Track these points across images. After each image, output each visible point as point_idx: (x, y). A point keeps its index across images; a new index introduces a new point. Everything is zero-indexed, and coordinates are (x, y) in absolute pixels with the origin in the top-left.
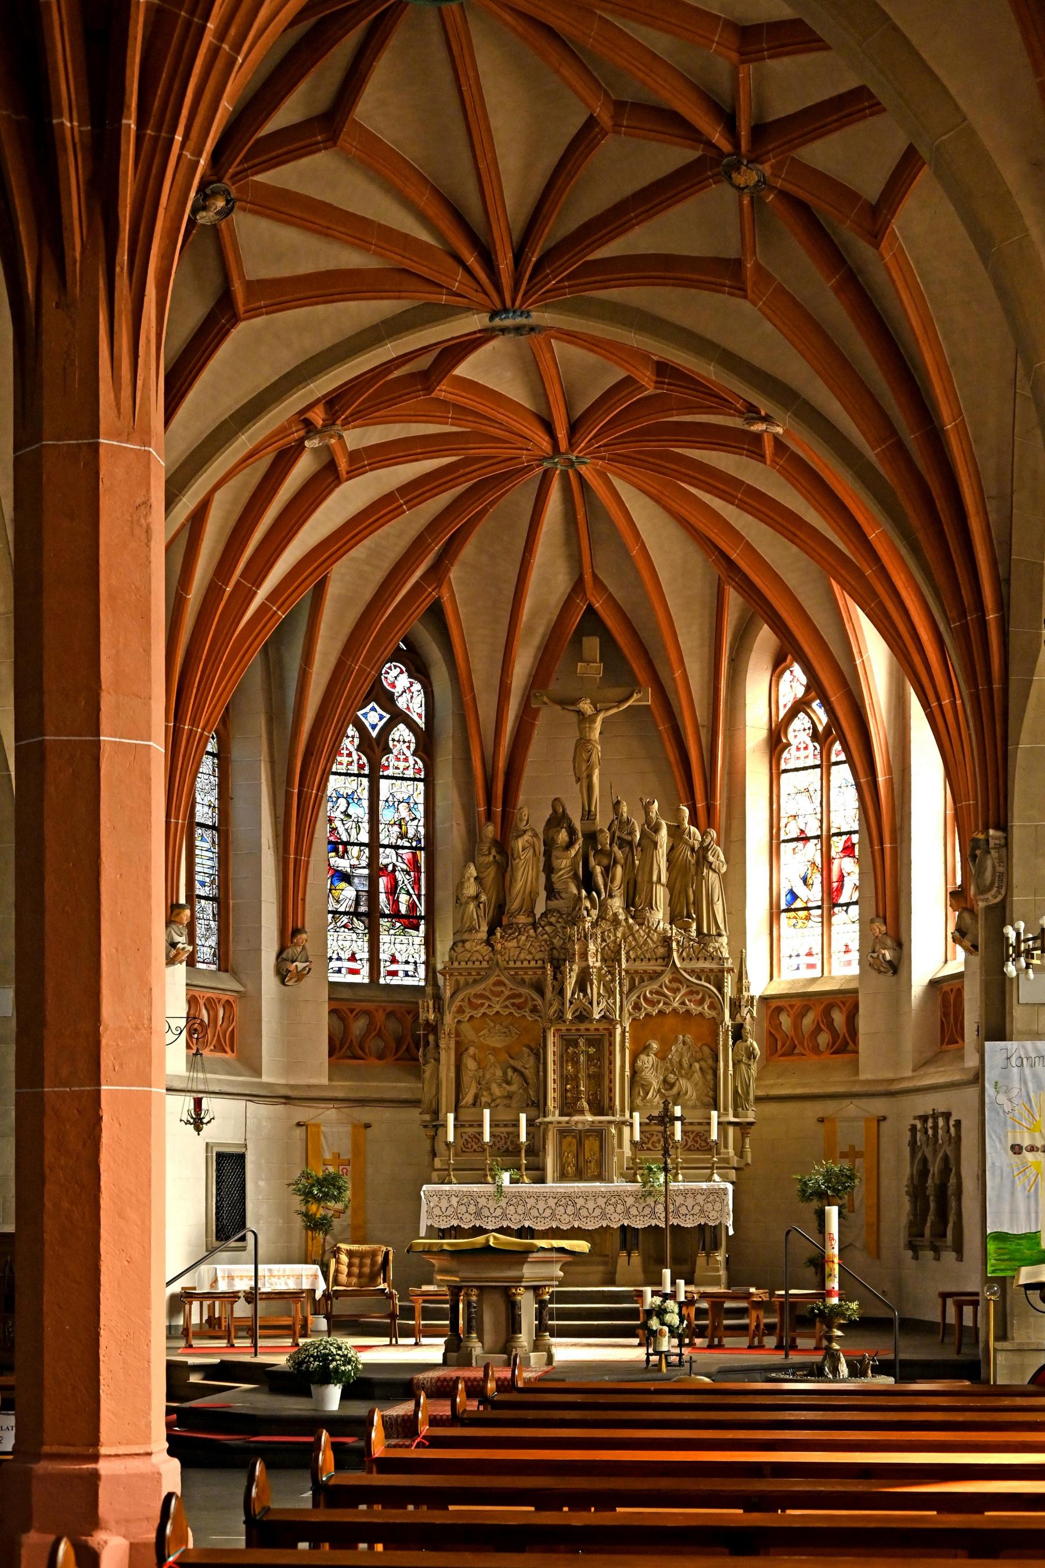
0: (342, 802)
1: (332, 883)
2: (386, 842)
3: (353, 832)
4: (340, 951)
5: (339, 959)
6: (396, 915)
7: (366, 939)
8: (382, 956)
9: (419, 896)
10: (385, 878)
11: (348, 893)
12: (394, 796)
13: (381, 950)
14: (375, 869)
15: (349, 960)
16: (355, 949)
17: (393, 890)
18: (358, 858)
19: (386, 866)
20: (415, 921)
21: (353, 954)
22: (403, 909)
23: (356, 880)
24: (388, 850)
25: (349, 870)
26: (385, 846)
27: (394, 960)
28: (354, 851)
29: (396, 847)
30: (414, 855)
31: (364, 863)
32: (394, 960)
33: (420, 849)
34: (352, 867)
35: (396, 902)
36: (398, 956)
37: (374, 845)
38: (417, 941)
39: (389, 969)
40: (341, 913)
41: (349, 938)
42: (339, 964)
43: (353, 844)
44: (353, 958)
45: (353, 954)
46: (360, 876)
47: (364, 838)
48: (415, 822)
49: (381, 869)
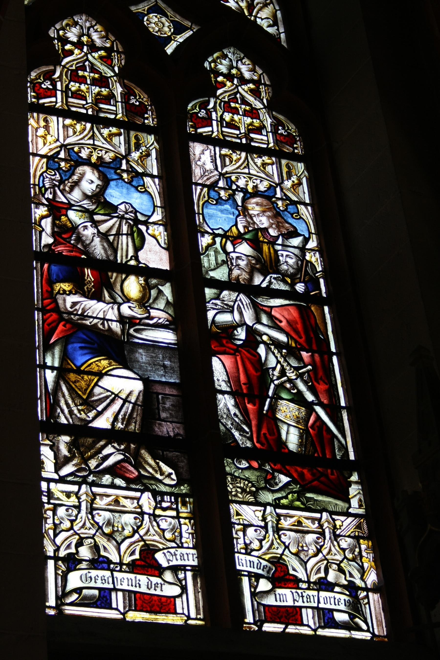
0: (90, 180)
1: (65, 357)
2: (220, 274)
3: (125, 243)
4: (101, 541)
5: (99, 562)
6: (270, 452)
7: (184, 511)
8: (243, 563)
9: (334, 411)
10: (228, 360)
11: (123, 384)
12: (229, 182)
13: (240, 545)
14: (198, 341)
15: (134, 568)
16: (153, 538)
17: (254, 387)
18: (143, 302)
19: (229, 330)
20: (333, 474)
21: (148, 552)
22: (292, 439)
23: (142, 356)
24: (227, 295)
25: (116, 327)
26: (220, 285)
27: (281, 577)
28: (133, 286)
29: (252, 291)
30: (304, 312)
31: (159, 314)
32: (281, 577)
33: (320, 301)
34: (122, 319)
35: (270, 422)
36: (292, 562)
37: (186, 274)
38: (346, 524)
39: (270, 601)
40: (101, 433)
41: (129, 505)
42: (101, 578)
43: (127, 270)
44: (146, 563)
45: (148, 552)
46: (153, 346)
47: (155, 256)
48: (296, 241)
49: (216, 337)
